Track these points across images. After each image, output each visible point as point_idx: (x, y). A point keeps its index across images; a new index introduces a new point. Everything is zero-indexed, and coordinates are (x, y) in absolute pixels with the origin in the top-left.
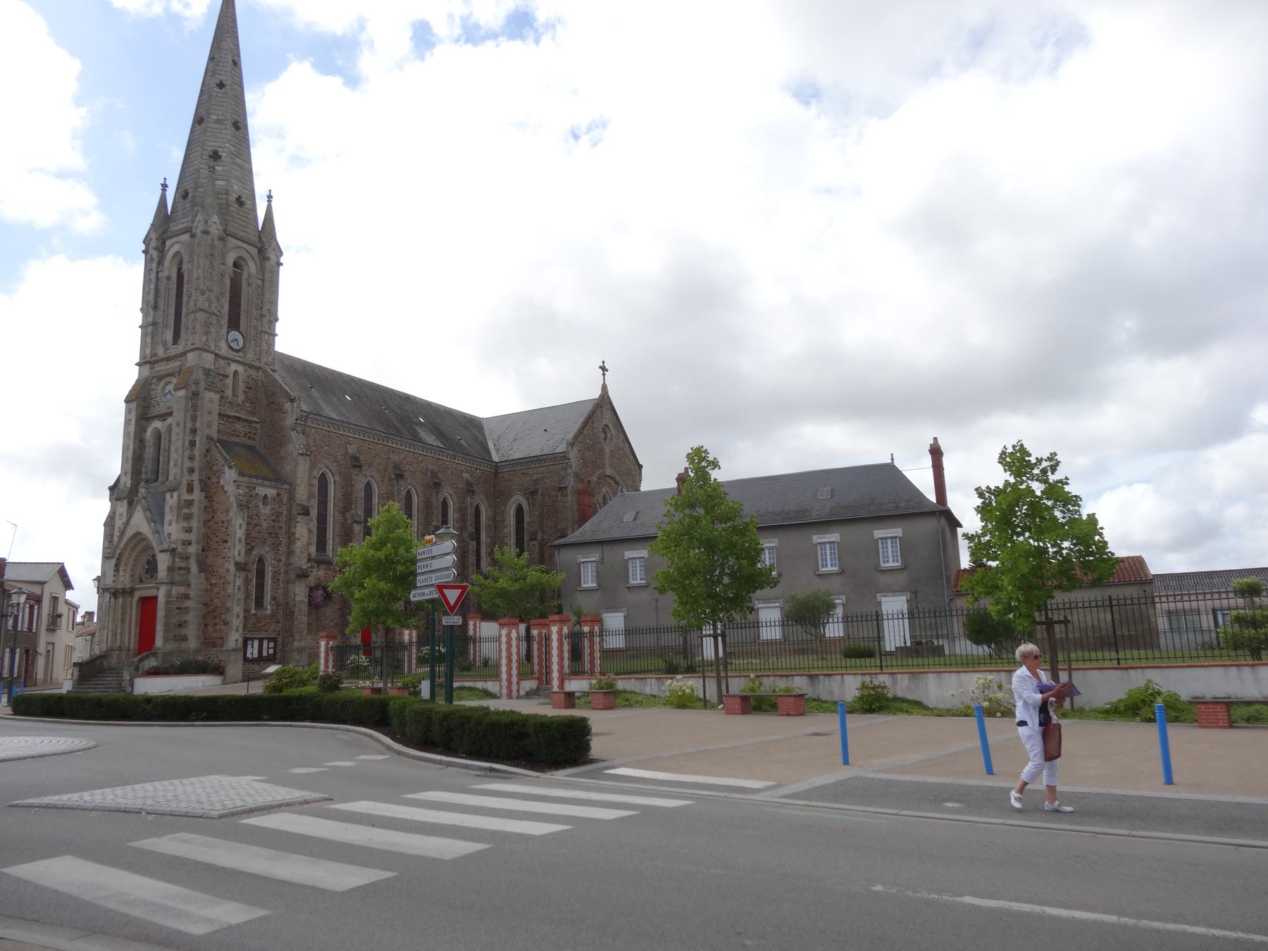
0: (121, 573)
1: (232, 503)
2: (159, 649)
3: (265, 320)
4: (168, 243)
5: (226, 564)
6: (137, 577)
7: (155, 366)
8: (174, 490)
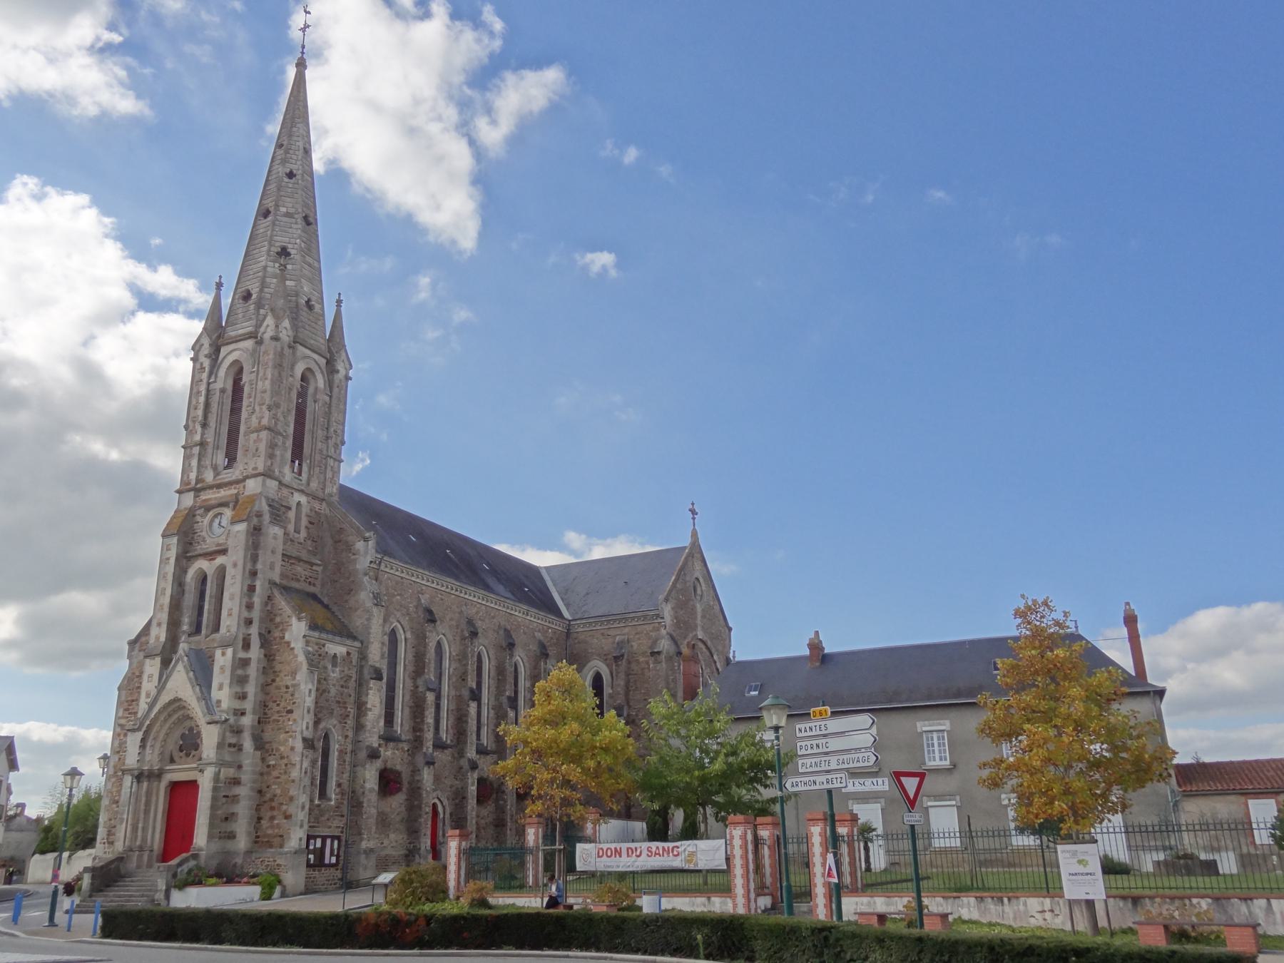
0: (148, 750)
1: (301, 663)
2: (201, 850)
3: (331, 442)
4: (224, 351)
5: (290, 740)
6: (167, 757)
7: (202, 493)
8: (228, 646)
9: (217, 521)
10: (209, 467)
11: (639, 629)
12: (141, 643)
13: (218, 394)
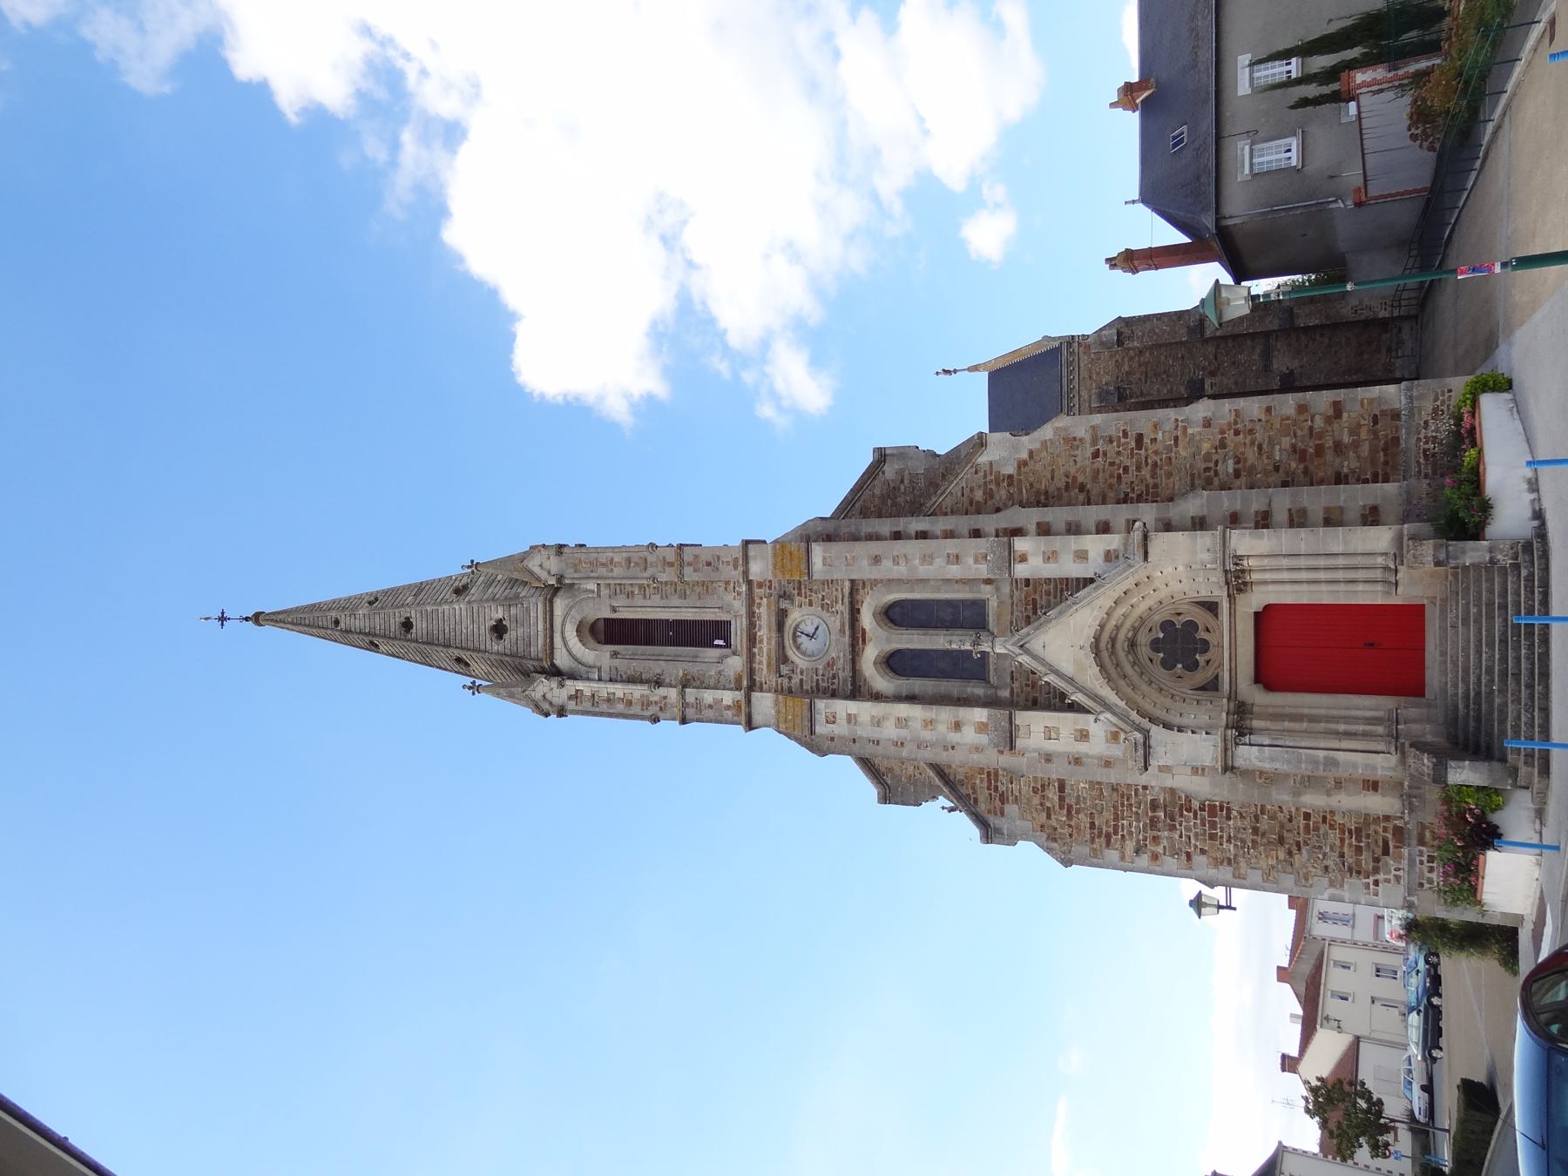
1: (1057, 429)
4: (562, 660)
5: (1190, 431)
6: (1203, 695)
9: (803, 639)
10: (721, 667)
11: (1084, 374)
12: (989, 812)
13: (616, 662)
